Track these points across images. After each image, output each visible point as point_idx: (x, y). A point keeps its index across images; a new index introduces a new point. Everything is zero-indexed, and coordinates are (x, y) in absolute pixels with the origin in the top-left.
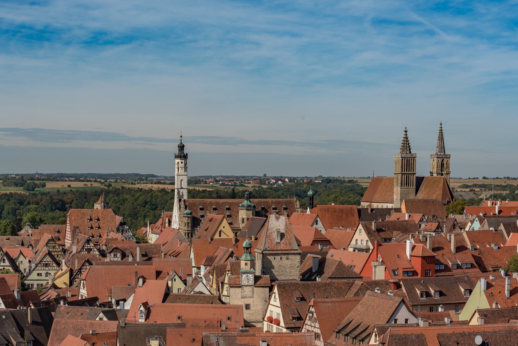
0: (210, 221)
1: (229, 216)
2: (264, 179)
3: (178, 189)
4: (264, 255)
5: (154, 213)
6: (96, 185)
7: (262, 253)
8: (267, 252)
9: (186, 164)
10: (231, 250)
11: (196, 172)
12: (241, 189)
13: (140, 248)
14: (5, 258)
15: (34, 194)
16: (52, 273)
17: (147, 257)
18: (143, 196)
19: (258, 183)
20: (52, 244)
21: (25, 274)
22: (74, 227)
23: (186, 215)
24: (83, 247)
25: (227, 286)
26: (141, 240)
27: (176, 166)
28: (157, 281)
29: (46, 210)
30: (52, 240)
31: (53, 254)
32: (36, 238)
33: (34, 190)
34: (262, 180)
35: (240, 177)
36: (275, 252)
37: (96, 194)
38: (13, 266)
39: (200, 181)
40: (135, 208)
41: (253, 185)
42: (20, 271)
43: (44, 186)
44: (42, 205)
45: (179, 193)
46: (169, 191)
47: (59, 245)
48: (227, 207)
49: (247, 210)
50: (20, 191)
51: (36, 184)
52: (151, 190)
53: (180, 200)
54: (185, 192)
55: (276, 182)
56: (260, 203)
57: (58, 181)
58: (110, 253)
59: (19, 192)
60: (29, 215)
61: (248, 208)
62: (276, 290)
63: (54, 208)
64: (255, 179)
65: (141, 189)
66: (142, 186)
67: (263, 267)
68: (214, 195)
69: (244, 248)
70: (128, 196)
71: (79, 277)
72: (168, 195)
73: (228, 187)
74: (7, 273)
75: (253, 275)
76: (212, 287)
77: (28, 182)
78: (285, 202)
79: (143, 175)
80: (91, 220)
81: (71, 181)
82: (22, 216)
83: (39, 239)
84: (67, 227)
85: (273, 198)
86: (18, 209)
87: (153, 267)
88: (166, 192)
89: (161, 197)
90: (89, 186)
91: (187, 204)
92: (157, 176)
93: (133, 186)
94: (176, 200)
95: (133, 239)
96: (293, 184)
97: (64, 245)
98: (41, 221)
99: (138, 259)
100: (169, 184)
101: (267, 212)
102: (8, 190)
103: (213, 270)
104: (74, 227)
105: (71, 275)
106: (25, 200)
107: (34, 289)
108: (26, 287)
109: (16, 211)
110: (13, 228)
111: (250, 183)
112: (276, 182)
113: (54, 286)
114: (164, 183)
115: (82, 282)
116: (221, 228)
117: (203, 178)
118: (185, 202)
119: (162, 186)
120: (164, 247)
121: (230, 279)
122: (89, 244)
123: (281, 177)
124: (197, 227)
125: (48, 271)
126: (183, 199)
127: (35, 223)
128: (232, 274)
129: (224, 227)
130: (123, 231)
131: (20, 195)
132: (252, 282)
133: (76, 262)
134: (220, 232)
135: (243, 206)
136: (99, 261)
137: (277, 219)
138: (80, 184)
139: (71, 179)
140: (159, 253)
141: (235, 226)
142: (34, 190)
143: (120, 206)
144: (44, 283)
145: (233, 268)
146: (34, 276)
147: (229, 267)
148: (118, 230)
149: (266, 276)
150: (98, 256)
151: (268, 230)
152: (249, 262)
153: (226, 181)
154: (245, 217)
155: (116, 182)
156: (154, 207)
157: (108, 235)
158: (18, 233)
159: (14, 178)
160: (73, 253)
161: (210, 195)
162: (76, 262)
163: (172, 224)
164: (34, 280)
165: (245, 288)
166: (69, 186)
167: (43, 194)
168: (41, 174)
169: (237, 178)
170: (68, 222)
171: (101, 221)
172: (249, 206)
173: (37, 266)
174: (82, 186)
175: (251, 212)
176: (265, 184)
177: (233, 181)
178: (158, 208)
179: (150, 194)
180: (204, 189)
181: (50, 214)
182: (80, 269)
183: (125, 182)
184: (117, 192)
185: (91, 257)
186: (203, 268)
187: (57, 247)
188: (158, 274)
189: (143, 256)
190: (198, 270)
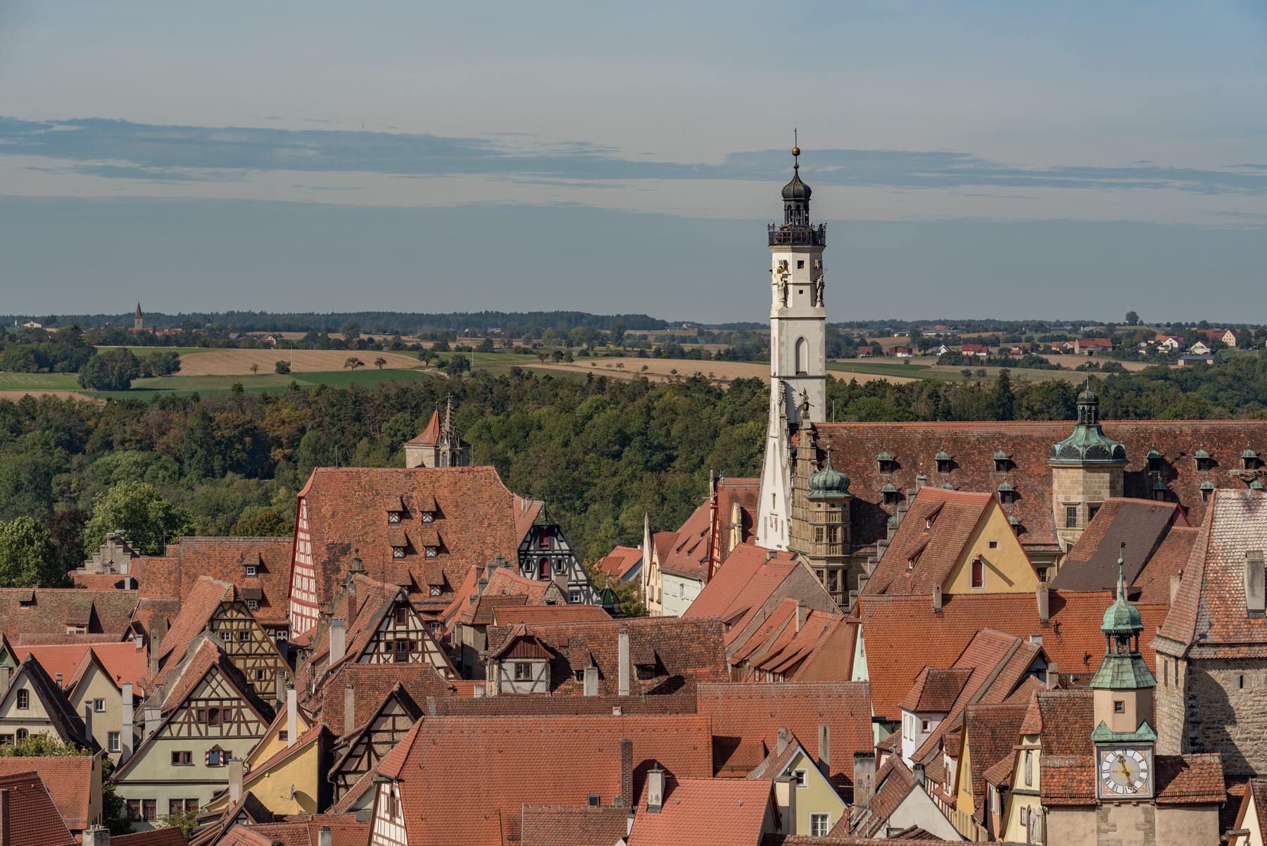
0: (933, 516)
1: (1011, 496)
2: (1131, 335)
3: (783, 380)
4: (1195, 668)
5: (661, 484)
6: (396, 361)
7: (1186, 658)
8: (1208, 653)
9: (816, 271)
10: (1034, 643)
11: (856, 305)
12: (1036, 377)
13: (633, 640)
14: (28, 685)
15: (131, 405)
16: (240, 749)
17: (664, 676)
18: (611, 412)
19: (1104, 352)
20: (234, 622)
21: (115, 758)
22: (330, 547)
23: (821, 494)
24: (377, 633)
25: (1036, 804)
26: (622, 604)
27: (776, 278)
28: (716, 781)
29: (181, 474)
30: (238, 602)
31: (239, 664)
32: (158, 598)
33: (126, 387)
34: (1121, 340)
35: (1027, 325)
36: (1244, 652)
37: (411, 406)
38: (63, 719)
39: (849, 342)
40: (577, 464)
41: (1083, 361)
42: (94, 747)
43: (172, 367)
44: (168, 450)
45: (787, 395)
46: (725, 387)
47: (266, 627)
48: (1001, 455)
49: (1088, 467)
50: (63, 389)
51: (136, 362)
52: (644, 385)
53: (793, 429)
54: (816, 392)
55: (1184, 348)
56: (1141, 439)
57: (232, 345)
58: (500, 658)
59: (63, 396)
60: (119, 495)
61: (1093, 460)
62: (1250, 819)
63: (217, 463)
64: (1089, 336)
65: (603, 380)
66: (603, 367)
67: (1192, 720)
68: (922, 407)
69: (1109, 634)
70: (544, 410)
71: (364, 766)
72: (720, 404)
73: (974, 369)
74: (39, 751)
75: (1148, 753)
76: (953, 807)
77: (102, 350)
78: (1252, 434)
79: (602, 321)
80: (404, 514)
81: (288, 345)
82: (75, 500)
83: (169, 599)
84: (301, 546)
85: (1176, 416)
86: (59, 470)
87: (698, 719)
88: (710, 391)
89: (691, 412)
90: (370, 365)
91: (825, 442)
92: (663, 325)
93: (562, 367)
94: (776, 427)
95: (588, 596)
96: (1257, 354)
97: (286, 628)
98: (173, 522)
99: (623, 688)
100: (719, 357)
101: (1173, 474)
102: (36, 388)
103: (960, 730)
104: (330, 547)
105: (326, 759)
106: (89, 432)
107: (159, 824)
108: (123, 813)
109: (48, 477)
110: (50, 552)
111: (1070, 352)
112: (1184, 348)
113: (255, 811)
114: (697, 355)
115: (386, 788)
116: (980, 548)
117: (864, 332)
118: (816, 437)
119: (688, 368)
120: (734, 630)
121: (1045, 770)
122: (401, 620)
123: (1204, 325)
124: (870, 541)
125: (226, 745)
126: (806, 424)
127: (146, 532)
128: (1047, 750)
129: (993, 545)
130: (543, 562)
131: (67, 410)
132: (1144, 784)
133: (350, 700)
134: (977, 565)
135: (1070, 452)
136: (449, 697)
137: (1250, 506)
138: (332, 361)
139: (287, 336)
140: (713, 660)
141: (1036, 537)
142: (126, 387)
143: (510, 454)
144: (204, 795)
145: (1051, 725)
146: (157, 762)
147: (1032, 721)
148: (523, 558)
149: (1207, 758)
150: (442, 672)
151: (1209, 556)
152: (1130, 699)
153: (967, 342)
154: (1077, 498)
155: (487, 347)
156: (658, 457)
157: (483, 583)
158: (72, 574)
159: (40, 335)
160: (332, 660)
161: (902, 404)
162: (350, 700)
163: (760, 532)
164: (155, 780)
165: (1114, 813)
166: (283, 369)
167: (171, 403)
168: (158, 316)
169: (1014, 331)
170: (303, 525)
171: (450, 523)
172: (1096, 452)
173: (169, 717)
174: (340, 367)
175: (1107, 476)
176: (1135, 357)
177: (995, 343)
178: (676, 464)
179: (641, 401)
180: (877, 378)
181: (202, 490)
182: (369, 732)
183: (526, 352)
184: (497, 396)
185: (415, 678)
186: (909, 722)
187: (258, 635)
188: (723, 750)
189: (644, 670)
190: (887, 735)
